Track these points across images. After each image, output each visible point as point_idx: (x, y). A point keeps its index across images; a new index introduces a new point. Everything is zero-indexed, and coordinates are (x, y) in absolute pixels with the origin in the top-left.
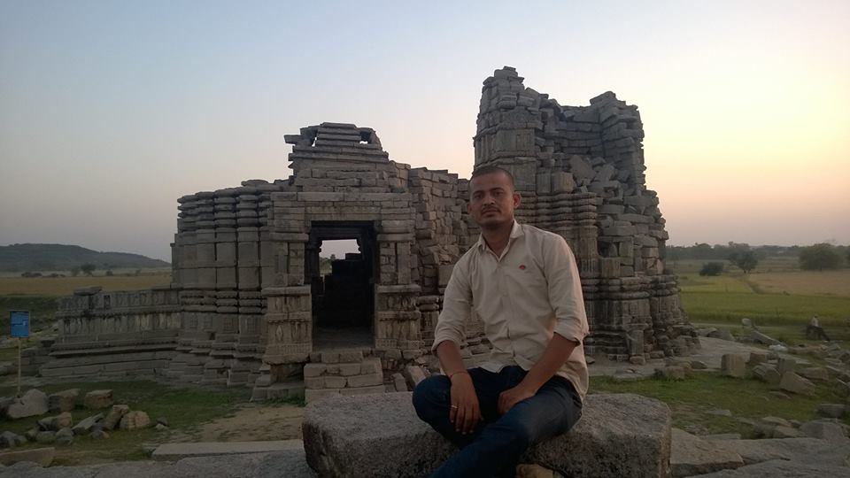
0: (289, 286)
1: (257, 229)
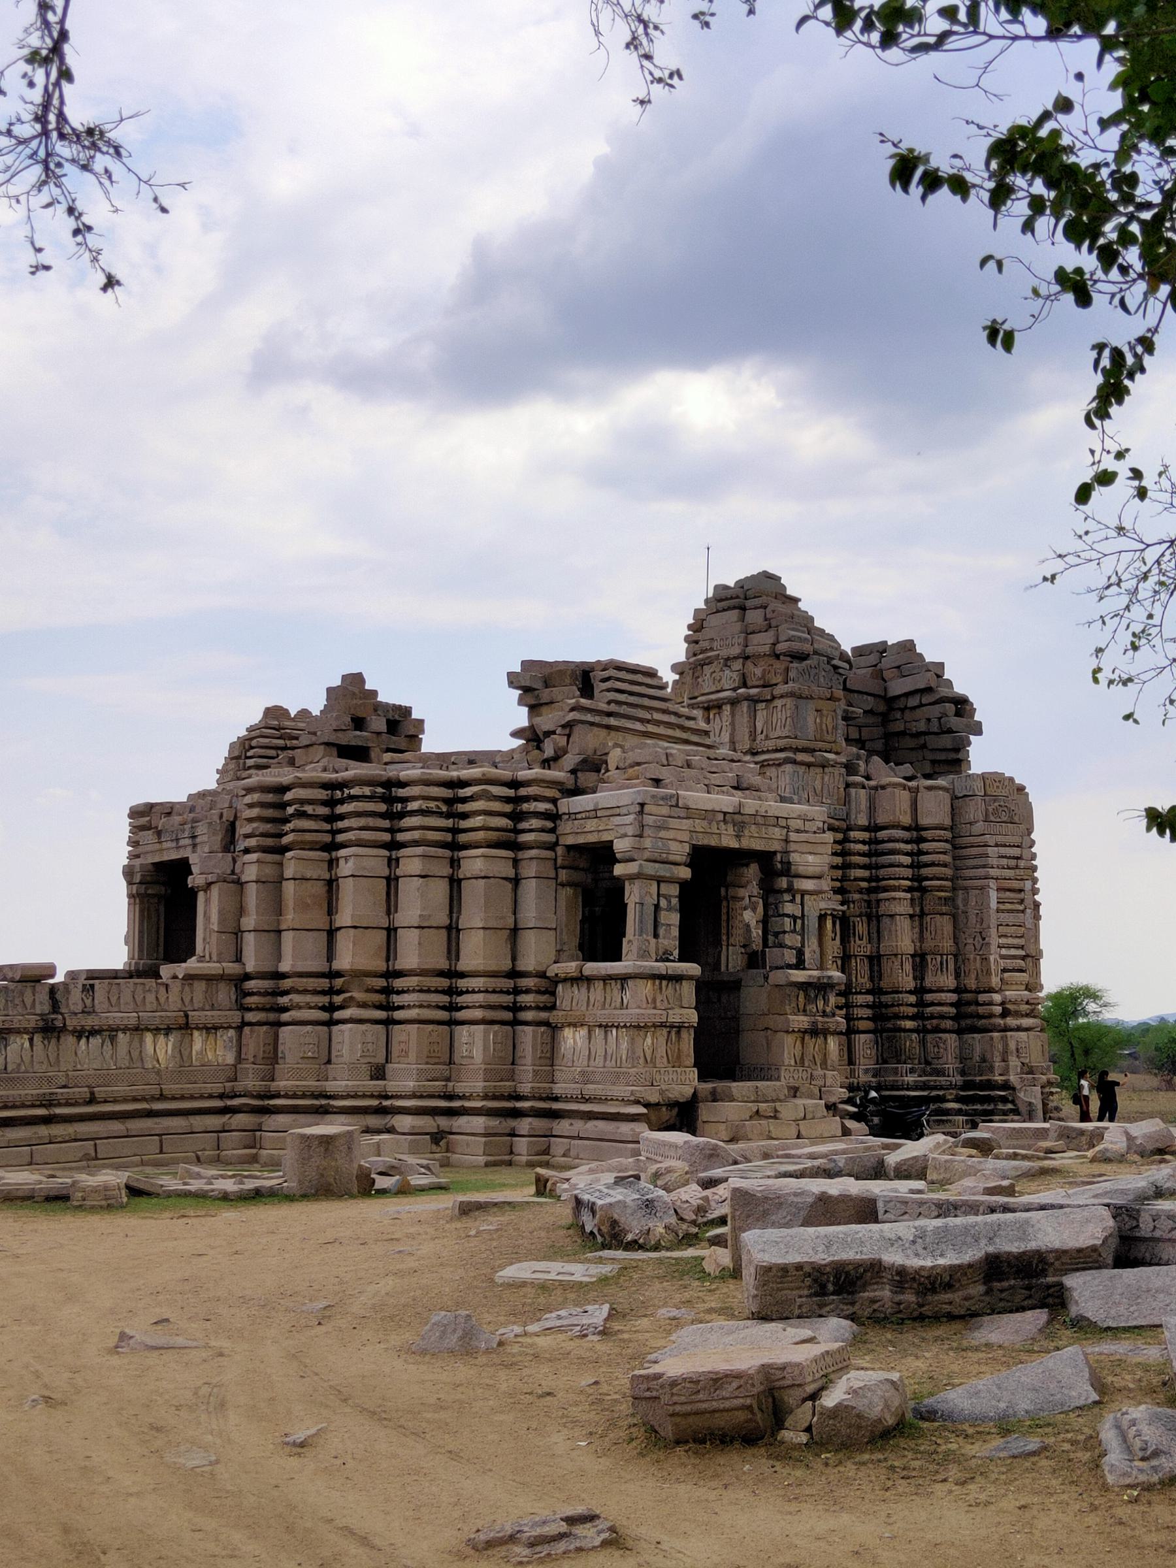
0: (657, 961)
1: (386, 853)
